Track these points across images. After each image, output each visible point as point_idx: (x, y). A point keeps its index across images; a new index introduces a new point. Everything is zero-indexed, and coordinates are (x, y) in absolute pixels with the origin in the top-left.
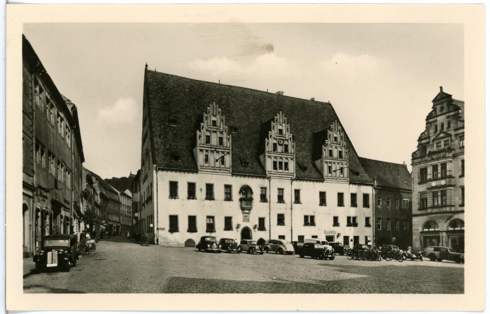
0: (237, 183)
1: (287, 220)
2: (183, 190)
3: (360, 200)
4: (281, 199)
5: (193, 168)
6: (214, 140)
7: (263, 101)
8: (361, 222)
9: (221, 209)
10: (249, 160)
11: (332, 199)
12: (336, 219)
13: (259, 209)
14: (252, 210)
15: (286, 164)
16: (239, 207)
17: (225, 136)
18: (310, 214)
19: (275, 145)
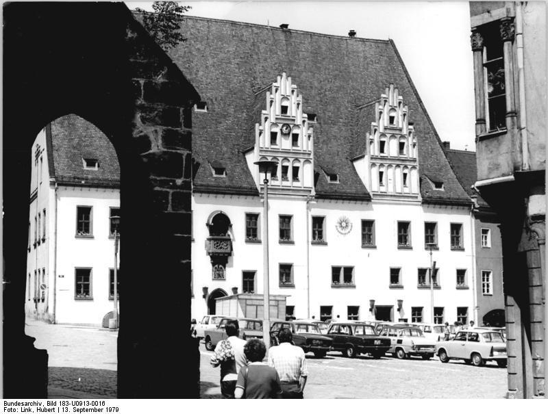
1: (298, 275)
3: (443, 235)
4: (285, 235)
7: (259, 47)
8: (447, 277)
11: (386, 234)
12: (395, 274)
15: (296, 170)
16: (205, 252)
19: (274, 136)
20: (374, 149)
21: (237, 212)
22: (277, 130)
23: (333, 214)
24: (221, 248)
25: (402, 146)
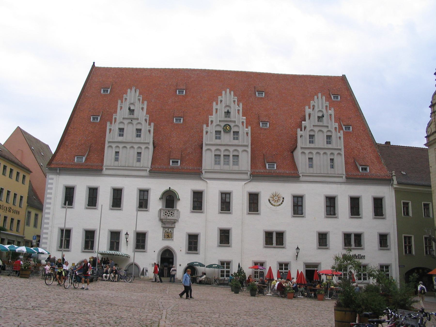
0: (157, 187)
1: (234, 237)
2: (80, 197)
3: (367, 207)
5: (95, 168)
6: (130, 133)
8: (371, 242)
9: (128, 219)
10: (176, 154)
11: (315, 204)
13: (187, 220)
16: (158, 219)
17: (145, 127)
18: (275, 228)
19: (218, 132)
20: (302, 142)
21: (184, 188)
24: (169, 216)
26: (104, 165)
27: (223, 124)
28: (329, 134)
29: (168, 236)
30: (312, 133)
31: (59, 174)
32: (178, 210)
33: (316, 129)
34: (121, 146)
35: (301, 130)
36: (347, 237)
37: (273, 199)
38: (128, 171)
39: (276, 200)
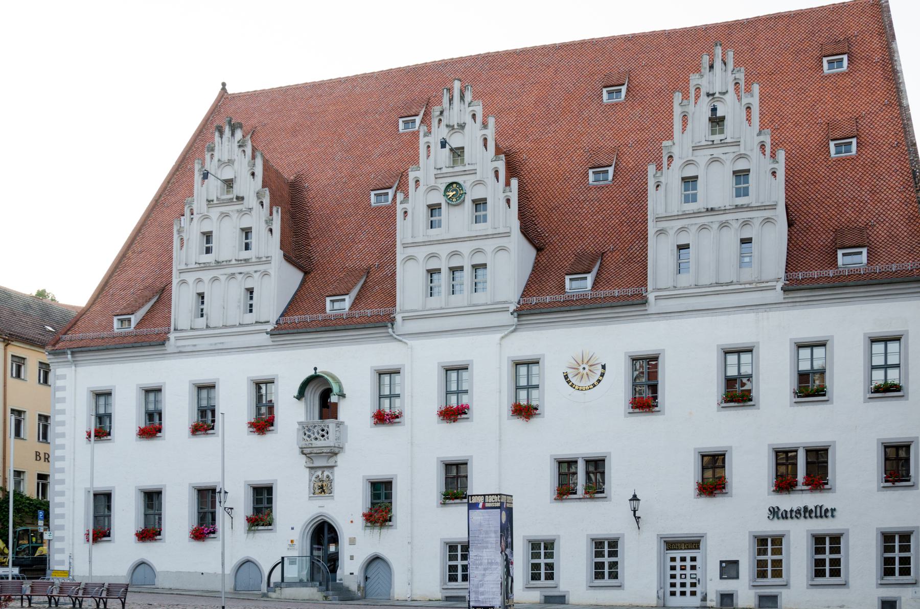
5: (151, 338)
14: (340, 458)
16: (298, 451)
19: (434, 209)
22: (437, 197)
23: (558, 344)
24: (316, 439)
25: (741, 175)
26: (172, 328)
27: (442, 184)
28: (741, 165)
29: (322, 489)
30: (690, 172)
31: (75, 363)
32: (339, 425)
33: (702, 157)
34: (206, 276)
35: (659, 168)
36: (784, 458)
37: (576, 372)
38: (221, 338)
39: (584, 375)
